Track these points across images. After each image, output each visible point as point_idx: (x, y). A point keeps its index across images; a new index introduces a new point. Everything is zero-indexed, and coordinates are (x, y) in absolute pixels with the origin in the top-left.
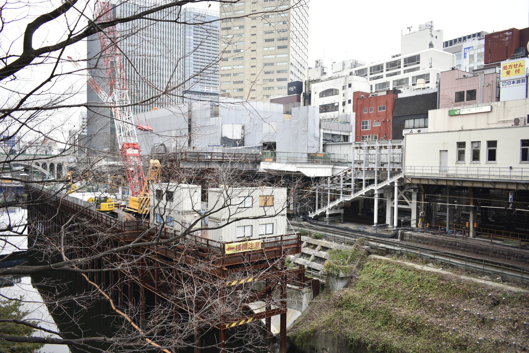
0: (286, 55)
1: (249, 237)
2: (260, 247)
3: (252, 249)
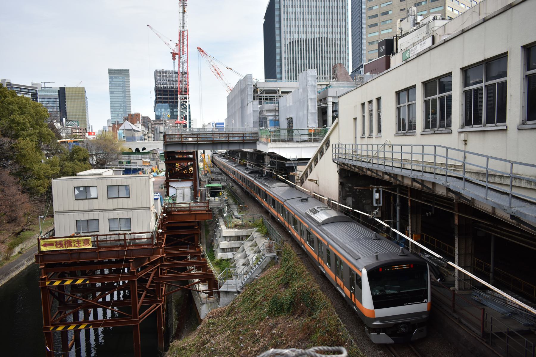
0: (442, 8)
3: (79, 246)
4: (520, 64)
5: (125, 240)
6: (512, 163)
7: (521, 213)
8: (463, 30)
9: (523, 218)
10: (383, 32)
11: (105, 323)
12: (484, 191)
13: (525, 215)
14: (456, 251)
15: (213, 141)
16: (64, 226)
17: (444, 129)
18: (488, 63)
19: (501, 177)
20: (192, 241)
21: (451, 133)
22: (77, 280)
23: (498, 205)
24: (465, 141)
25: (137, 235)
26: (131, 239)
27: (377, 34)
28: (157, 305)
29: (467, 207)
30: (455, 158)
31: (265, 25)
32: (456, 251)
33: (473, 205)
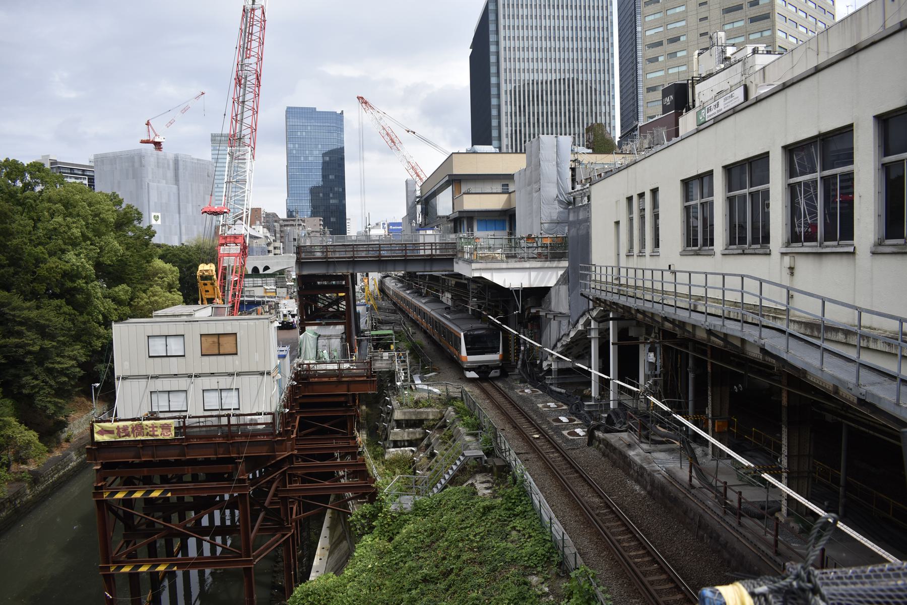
1: (155, 413)
2: (171, 435)
4: (872, 145)
5: (229, 425)
6: (860, 311)
7: (873, 395)
8: (784, 83)
9: (881, 406)
10: (671, 71)
11: (200, 563)
12: (817, 354)
13: (880, 398)
14: (785, 450)
15: (380, 256)
16: (131, 400)
17: (759, 246)
18: (824, 139)
19: (847, 333)
20: (344, 426)
21: (770, 254)
22: (152, 491)
23: (839, 380)
24: (792, 269)
25: (249, 417)
26: (238, 425)
27: (661, 73)
28: (284, 535)
29: (796, 378)
30: (775, 298)
31: (473, 59)
32: (785, 450)
33: (805, 377)
